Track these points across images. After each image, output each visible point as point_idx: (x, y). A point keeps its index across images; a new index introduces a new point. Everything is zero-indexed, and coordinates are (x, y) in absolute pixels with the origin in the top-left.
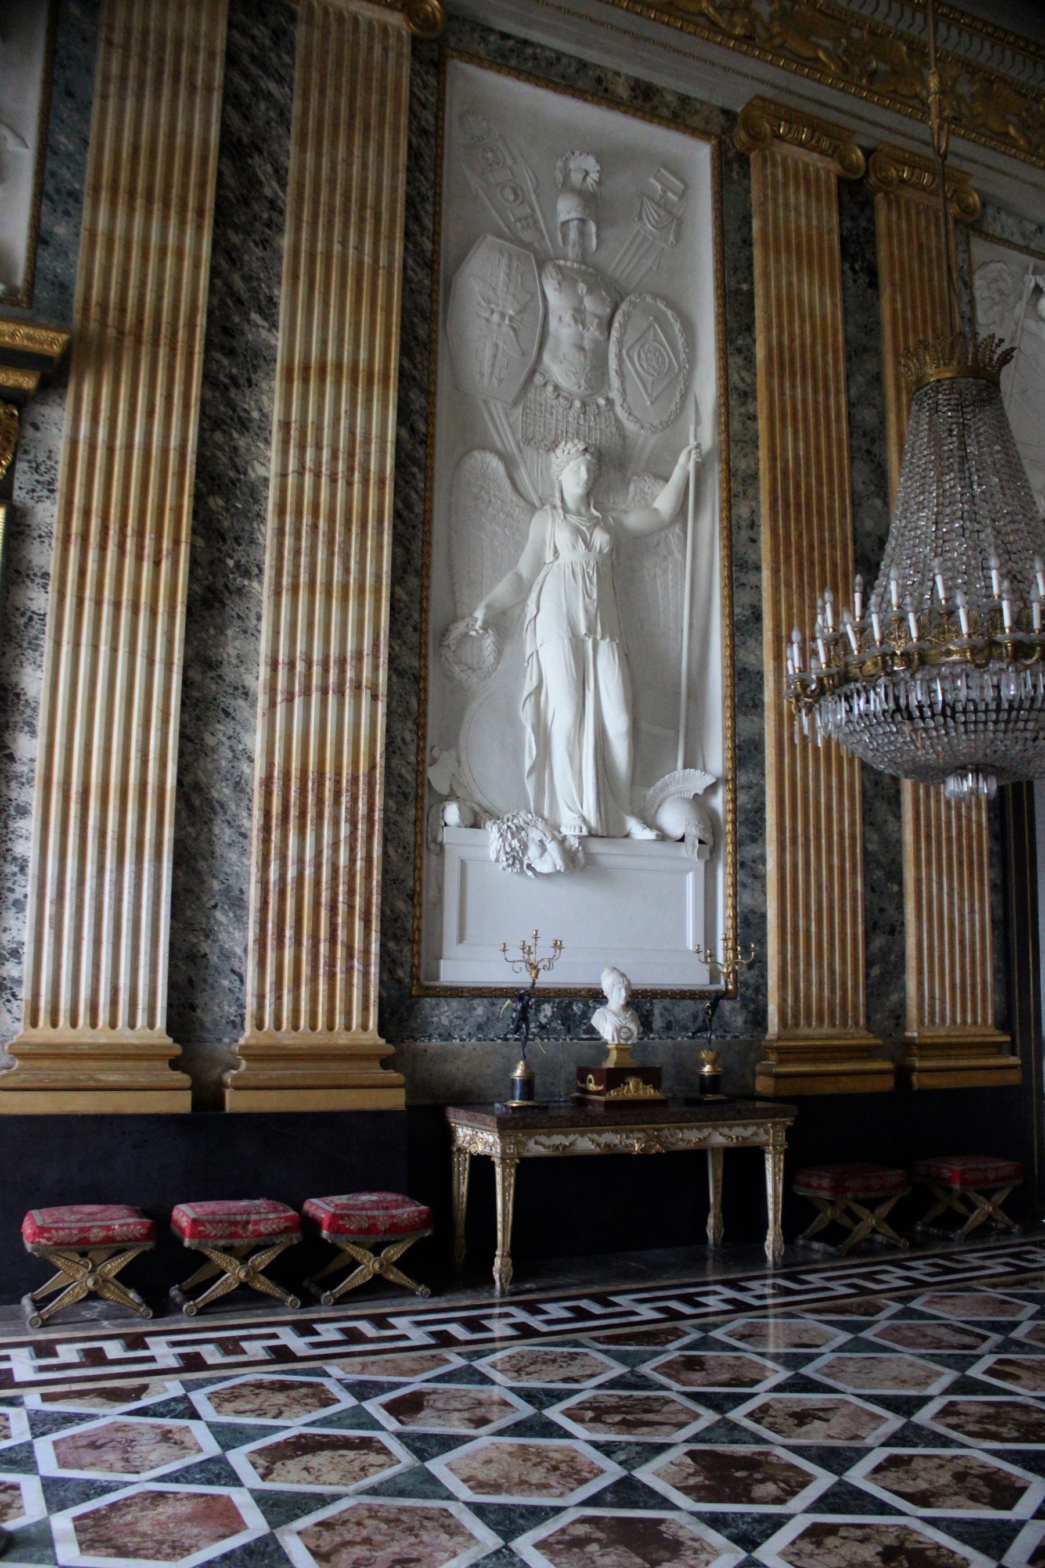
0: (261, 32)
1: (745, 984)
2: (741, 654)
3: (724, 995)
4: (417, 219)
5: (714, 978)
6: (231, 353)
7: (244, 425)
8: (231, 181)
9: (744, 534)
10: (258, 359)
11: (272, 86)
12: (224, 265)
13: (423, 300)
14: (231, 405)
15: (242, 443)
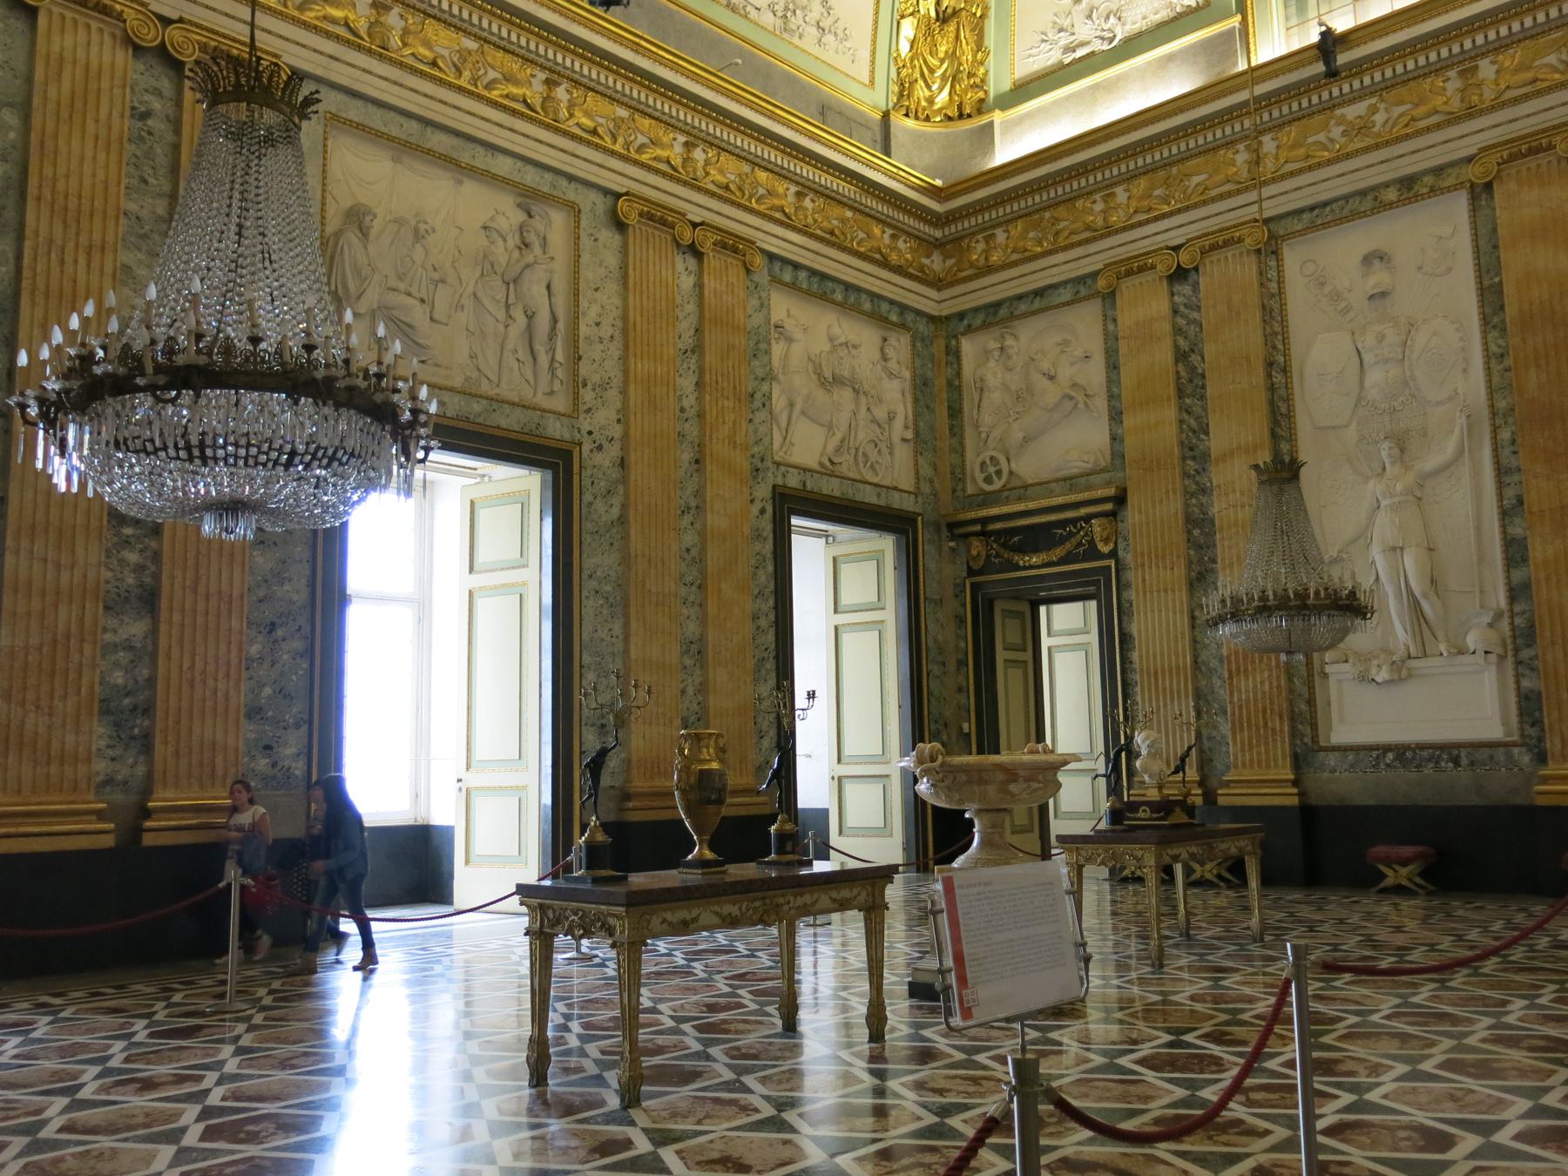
0: (1186, 289)
1: (1531, 737)
2: (1510, 530)
3: (1514, 744)
4: (1274, 347)
5: (1508, 734)
6: (1194, 458)
7: (1204, 491)
8: (1183, 374)
9: (1506, 452)
10: (1204, 458)
11: (1195, 315)
12: (1185, 416)
13: (1283, 392)
14: (1197, 483)
15: (1204, 500)
